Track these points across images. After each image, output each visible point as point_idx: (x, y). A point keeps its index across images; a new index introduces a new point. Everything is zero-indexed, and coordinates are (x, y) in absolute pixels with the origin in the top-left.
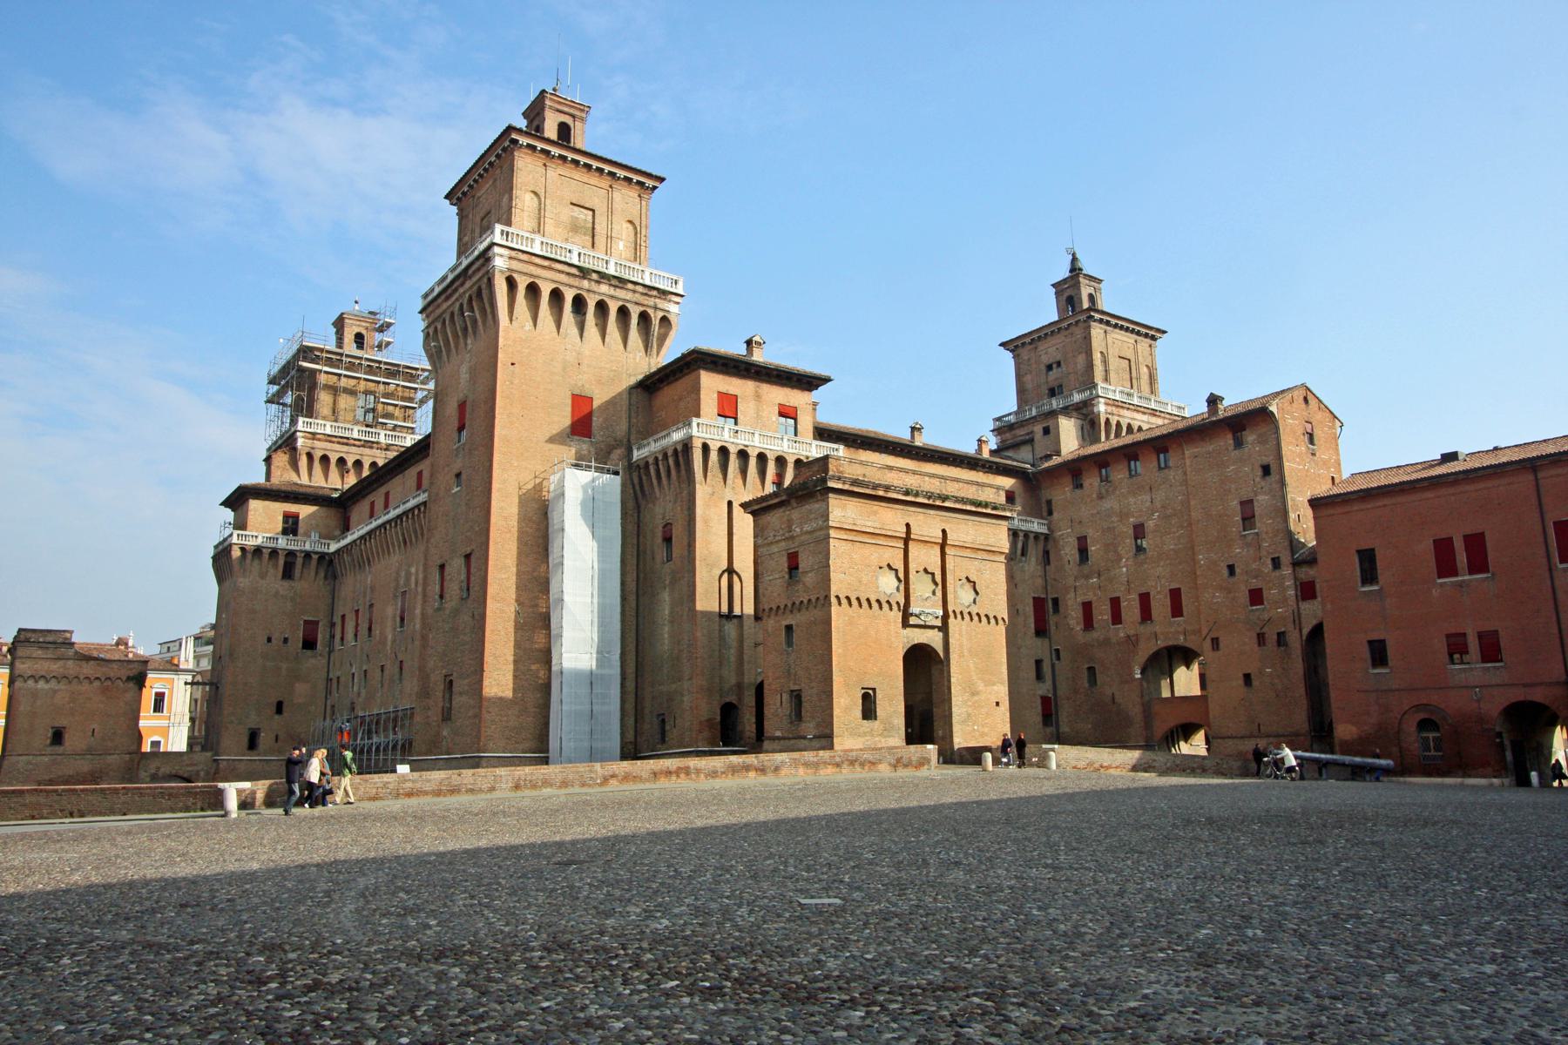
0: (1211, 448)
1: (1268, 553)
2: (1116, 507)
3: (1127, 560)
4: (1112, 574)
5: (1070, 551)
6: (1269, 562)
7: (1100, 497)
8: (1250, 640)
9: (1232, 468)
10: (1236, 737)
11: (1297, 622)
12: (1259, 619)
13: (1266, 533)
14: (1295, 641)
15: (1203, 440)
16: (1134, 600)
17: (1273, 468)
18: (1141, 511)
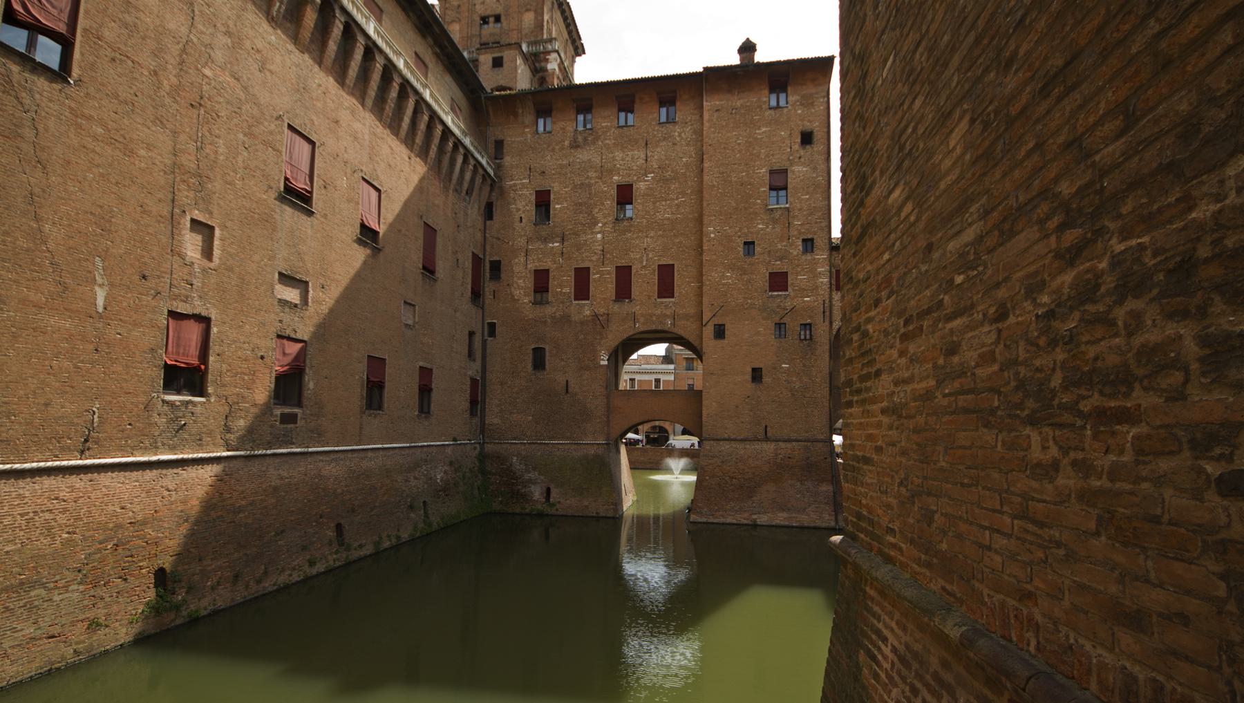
0: (739, 104)
1: (800, 233)
2: (597, 160)
3: (604, 224)
4: (583, 238)
5: (522, 205)
6: (800, 243)
7: (575, 145)
8: (765, 329)
9: (764, 129)
10: (735, 440)
11: (827, 314)
12: (779, 306)
13: (800, 210)
14: (822, 333)
15: (729, 91)
16: (609, 273)
17: (818, 135)
18: (630, 169)
